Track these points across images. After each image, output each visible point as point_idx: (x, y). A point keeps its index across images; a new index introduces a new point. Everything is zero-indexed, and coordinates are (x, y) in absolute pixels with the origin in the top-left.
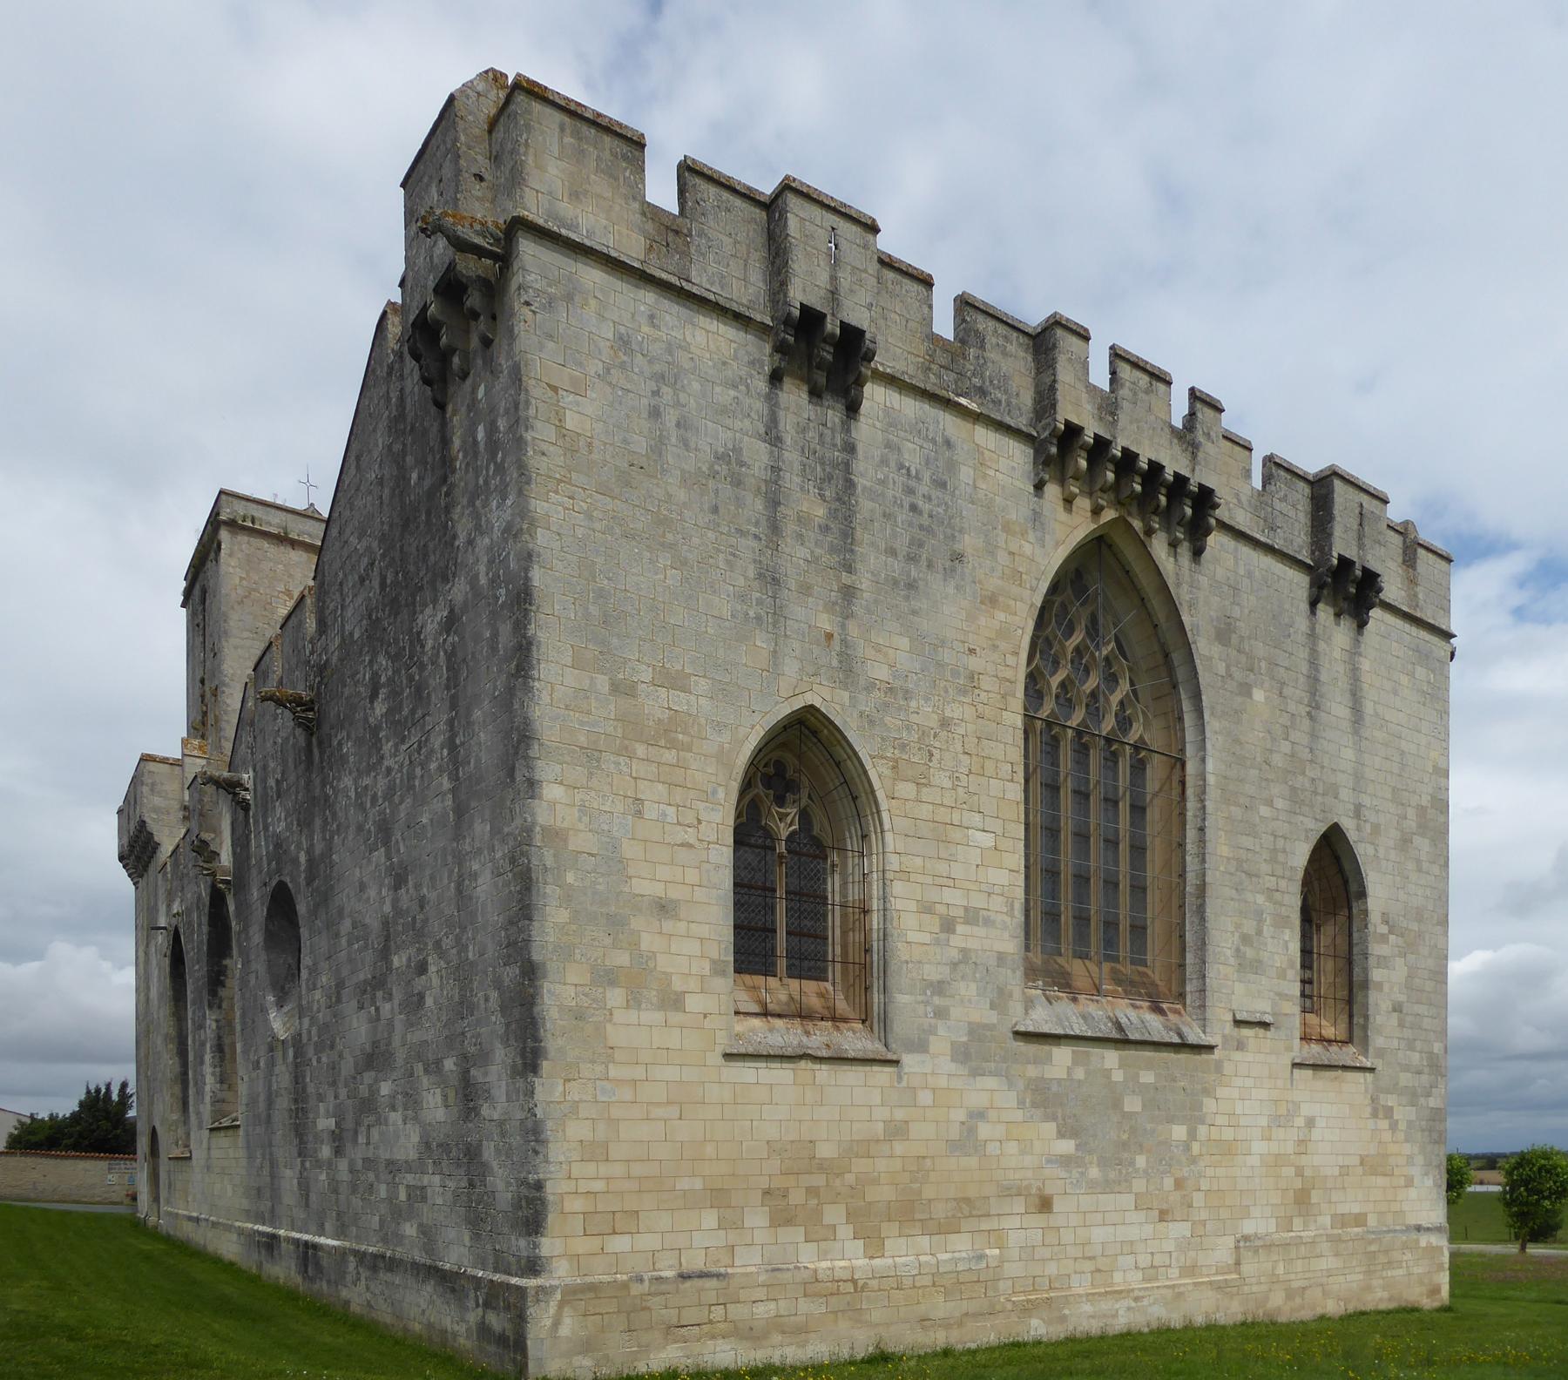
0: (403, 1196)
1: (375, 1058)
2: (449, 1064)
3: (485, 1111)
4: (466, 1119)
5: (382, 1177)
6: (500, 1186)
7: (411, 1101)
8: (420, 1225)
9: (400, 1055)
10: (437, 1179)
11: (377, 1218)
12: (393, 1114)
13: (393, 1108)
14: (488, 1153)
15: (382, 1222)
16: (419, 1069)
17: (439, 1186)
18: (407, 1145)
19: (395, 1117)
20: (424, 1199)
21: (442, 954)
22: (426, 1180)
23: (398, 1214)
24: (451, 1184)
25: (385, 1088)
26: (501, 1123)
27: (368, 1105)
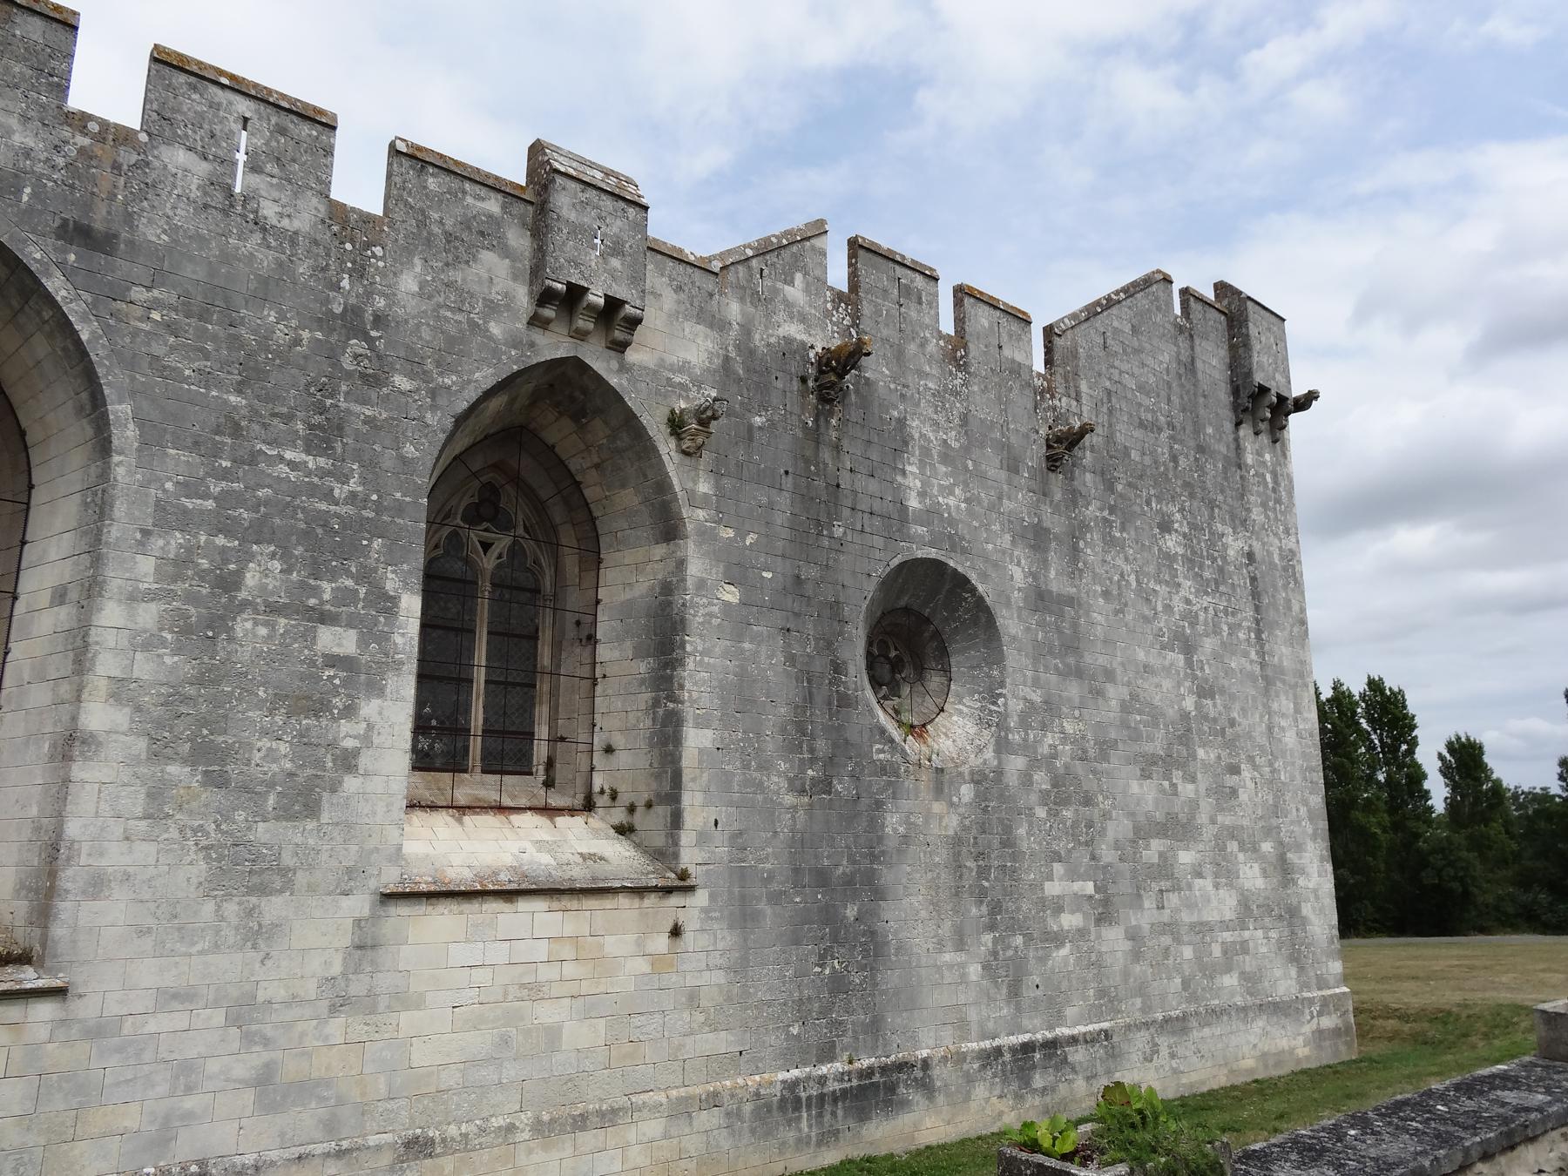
0: (1217, 951)
1: (1177, 828)
2: (1267, 847)
3: (1300, 882)
4: (1285, 886)
5: (1186, 938)
6: (1317, 930)
7: (1225, 873)
8: (1242, 973)
9: (1209, 832)
10: (1260, 933)
11: (1178, 981)
12: (1198, 882)
13: (1200, 875)
14: (1306, 910)
15: (1186, 984)
16: (1233, 846)
17: (1262, 940)
18: (1223, 905)
19: (1206, 884)
20: (1245, 951)
21: (1255, 767)
22: (1246, 934)
23: (1211, 971)
24: (1273, 934)
25: (1186, 857)
26: (1315, 891)
27: (1164, 869)
